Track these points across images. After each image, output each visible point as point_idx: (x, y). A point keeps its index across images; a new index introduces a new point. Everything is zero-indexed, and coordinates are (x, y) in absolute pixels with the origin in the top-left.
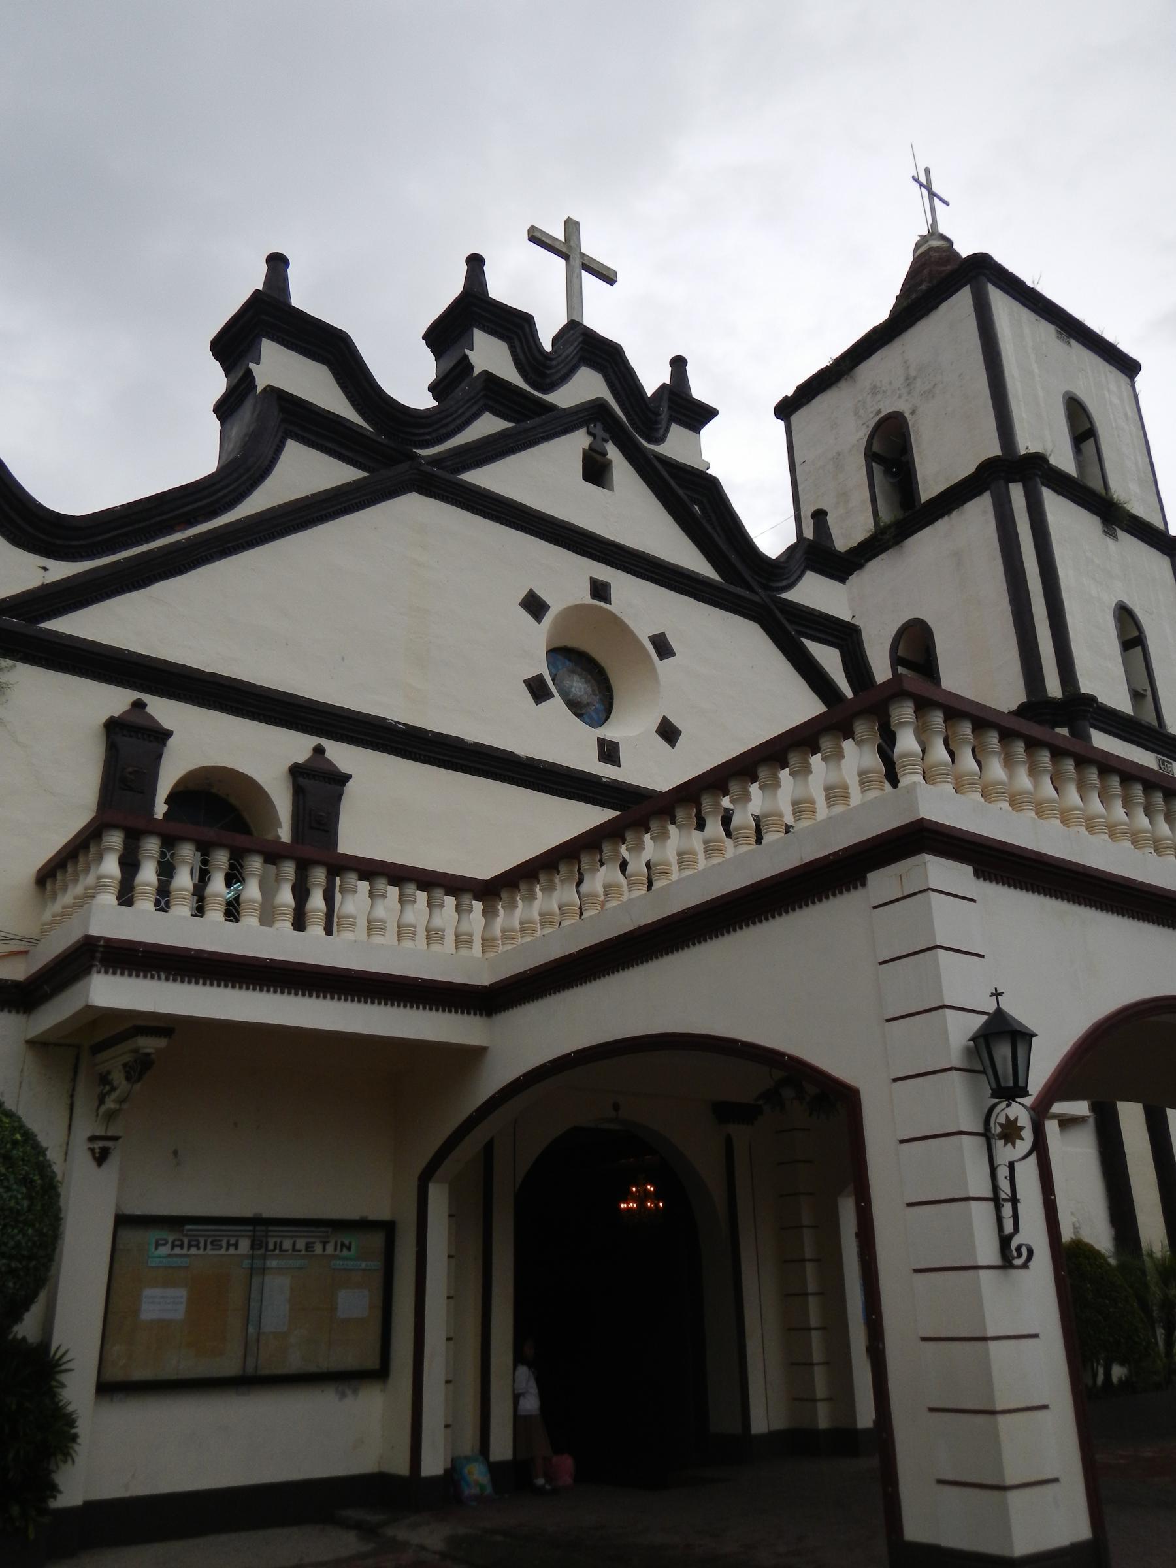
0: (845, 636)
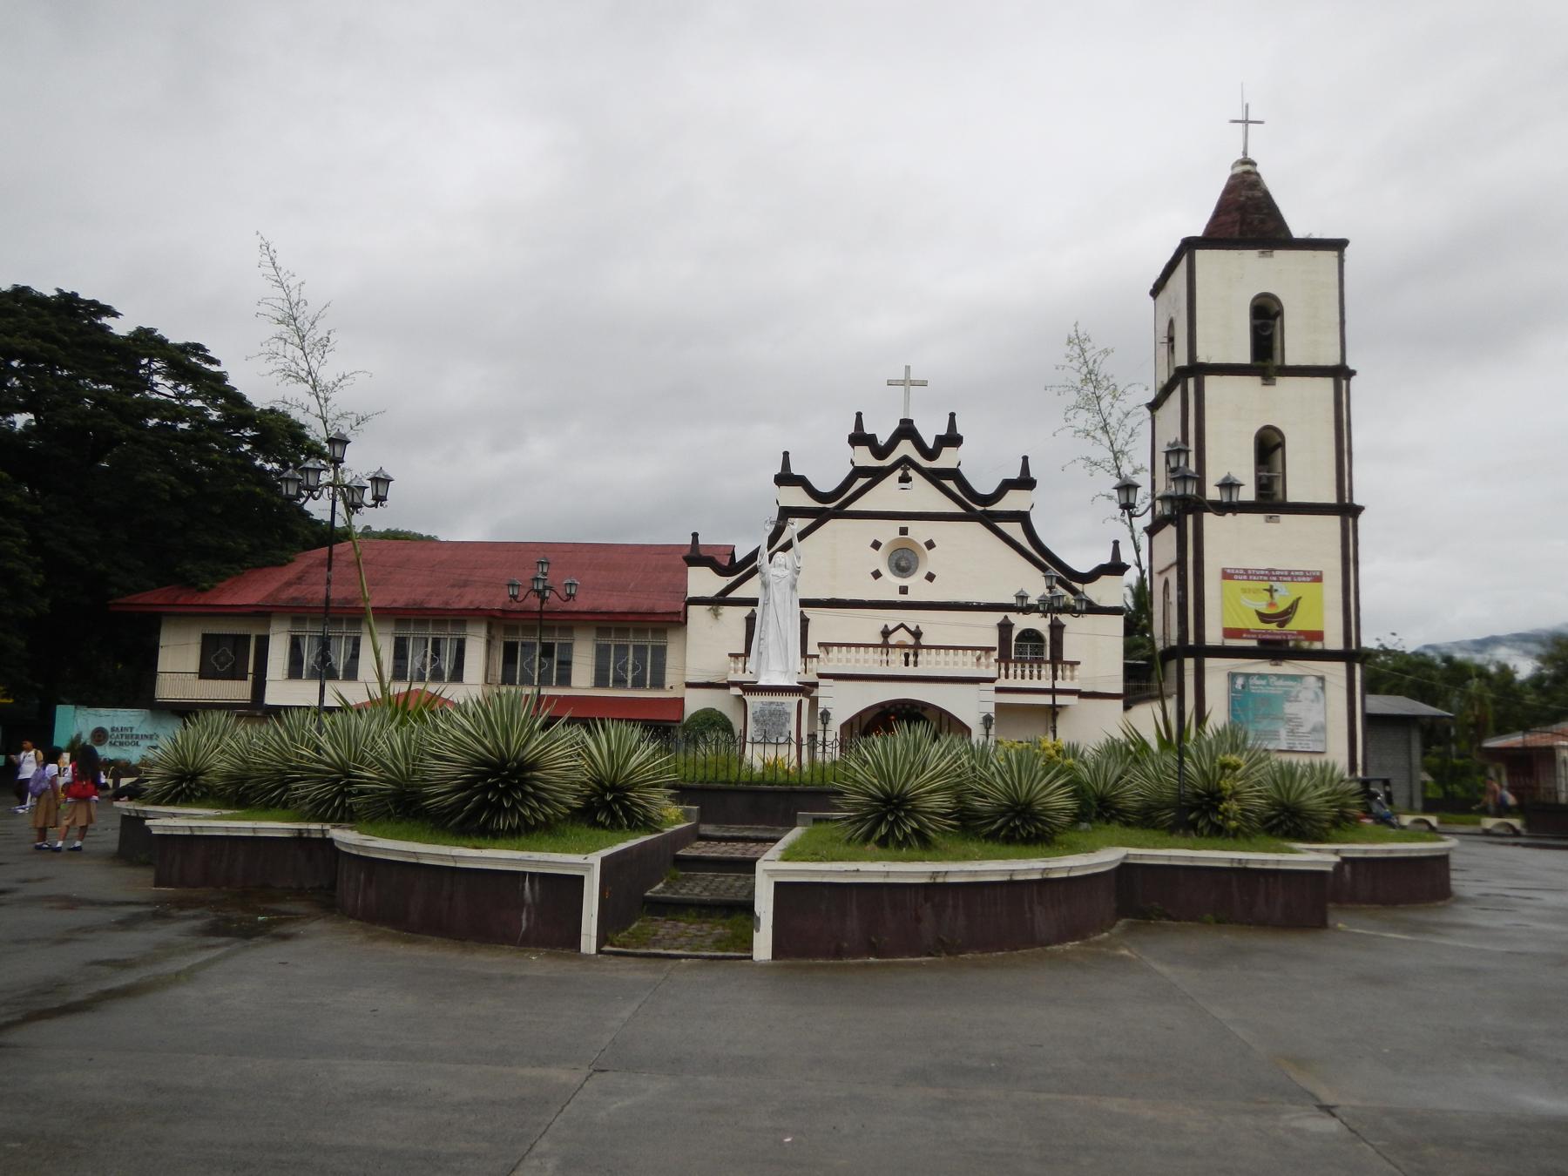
0: (1023, 518)
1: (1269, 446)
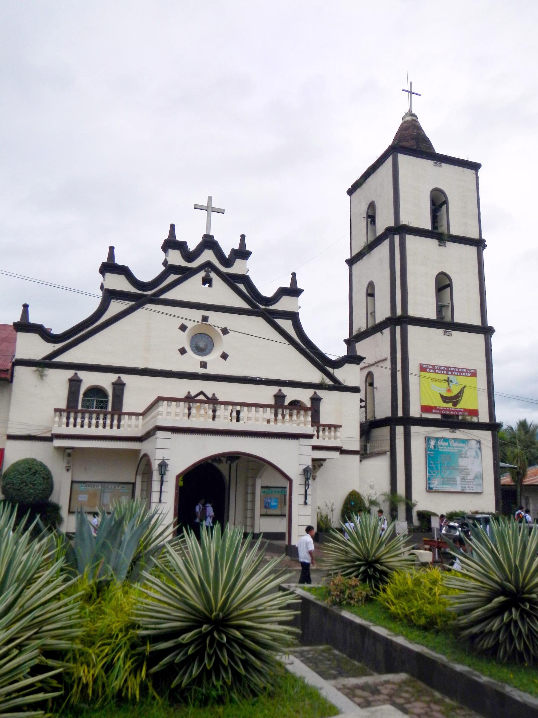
1: (443, 284)
